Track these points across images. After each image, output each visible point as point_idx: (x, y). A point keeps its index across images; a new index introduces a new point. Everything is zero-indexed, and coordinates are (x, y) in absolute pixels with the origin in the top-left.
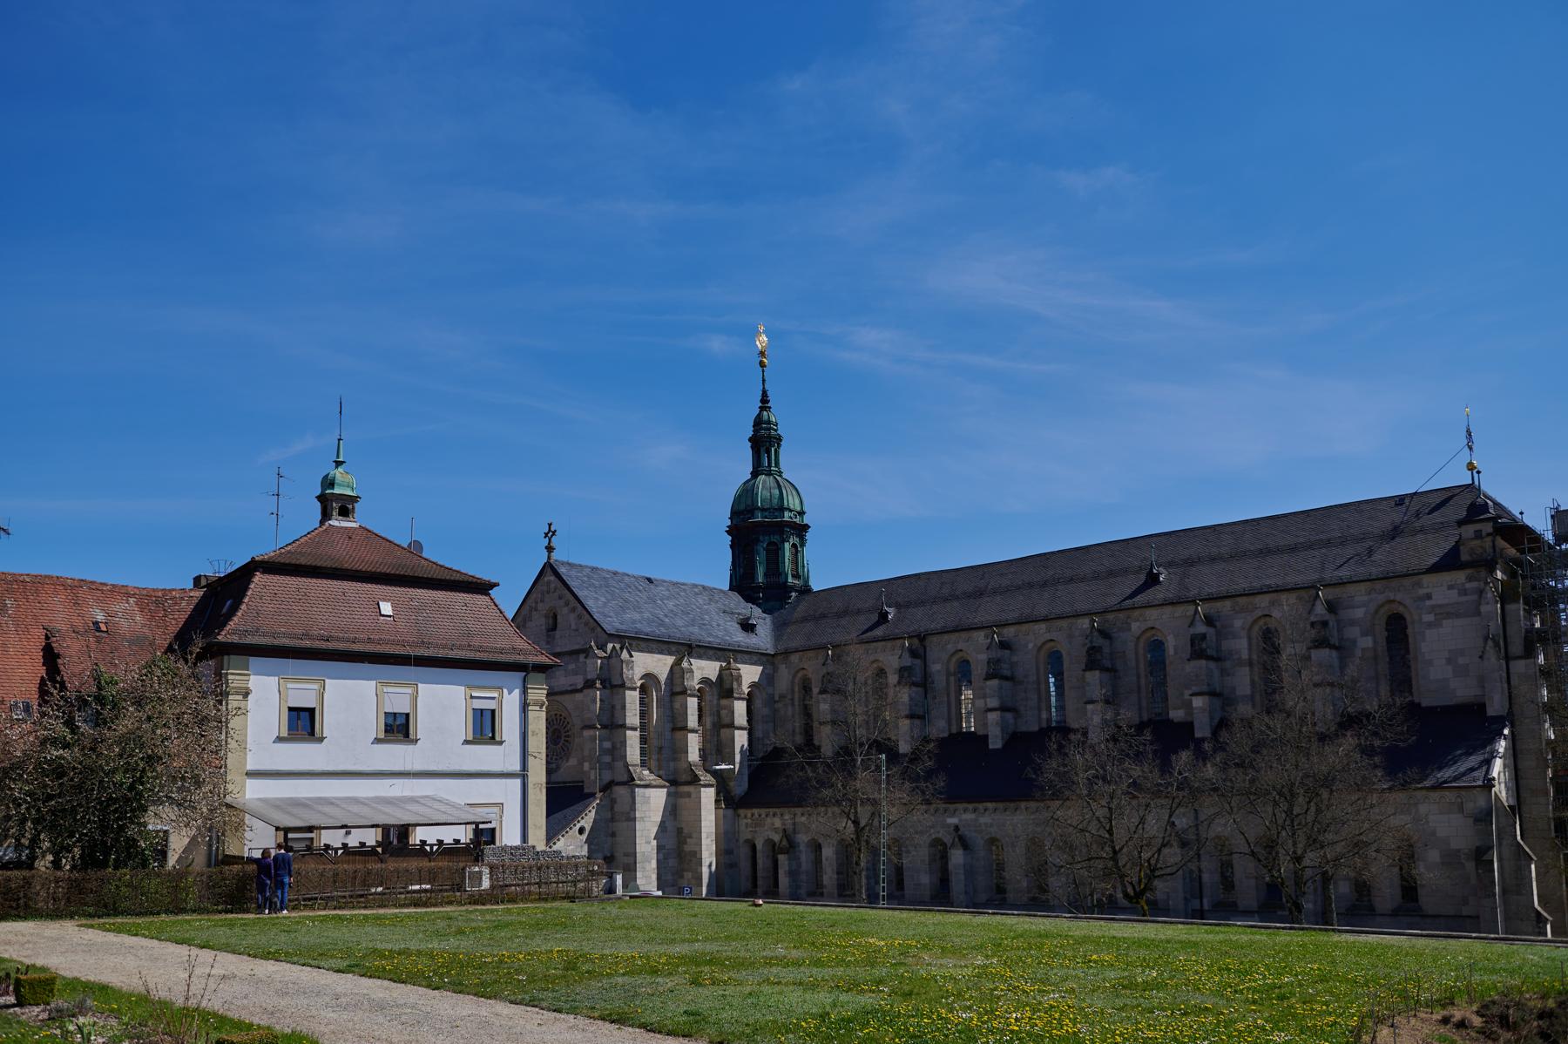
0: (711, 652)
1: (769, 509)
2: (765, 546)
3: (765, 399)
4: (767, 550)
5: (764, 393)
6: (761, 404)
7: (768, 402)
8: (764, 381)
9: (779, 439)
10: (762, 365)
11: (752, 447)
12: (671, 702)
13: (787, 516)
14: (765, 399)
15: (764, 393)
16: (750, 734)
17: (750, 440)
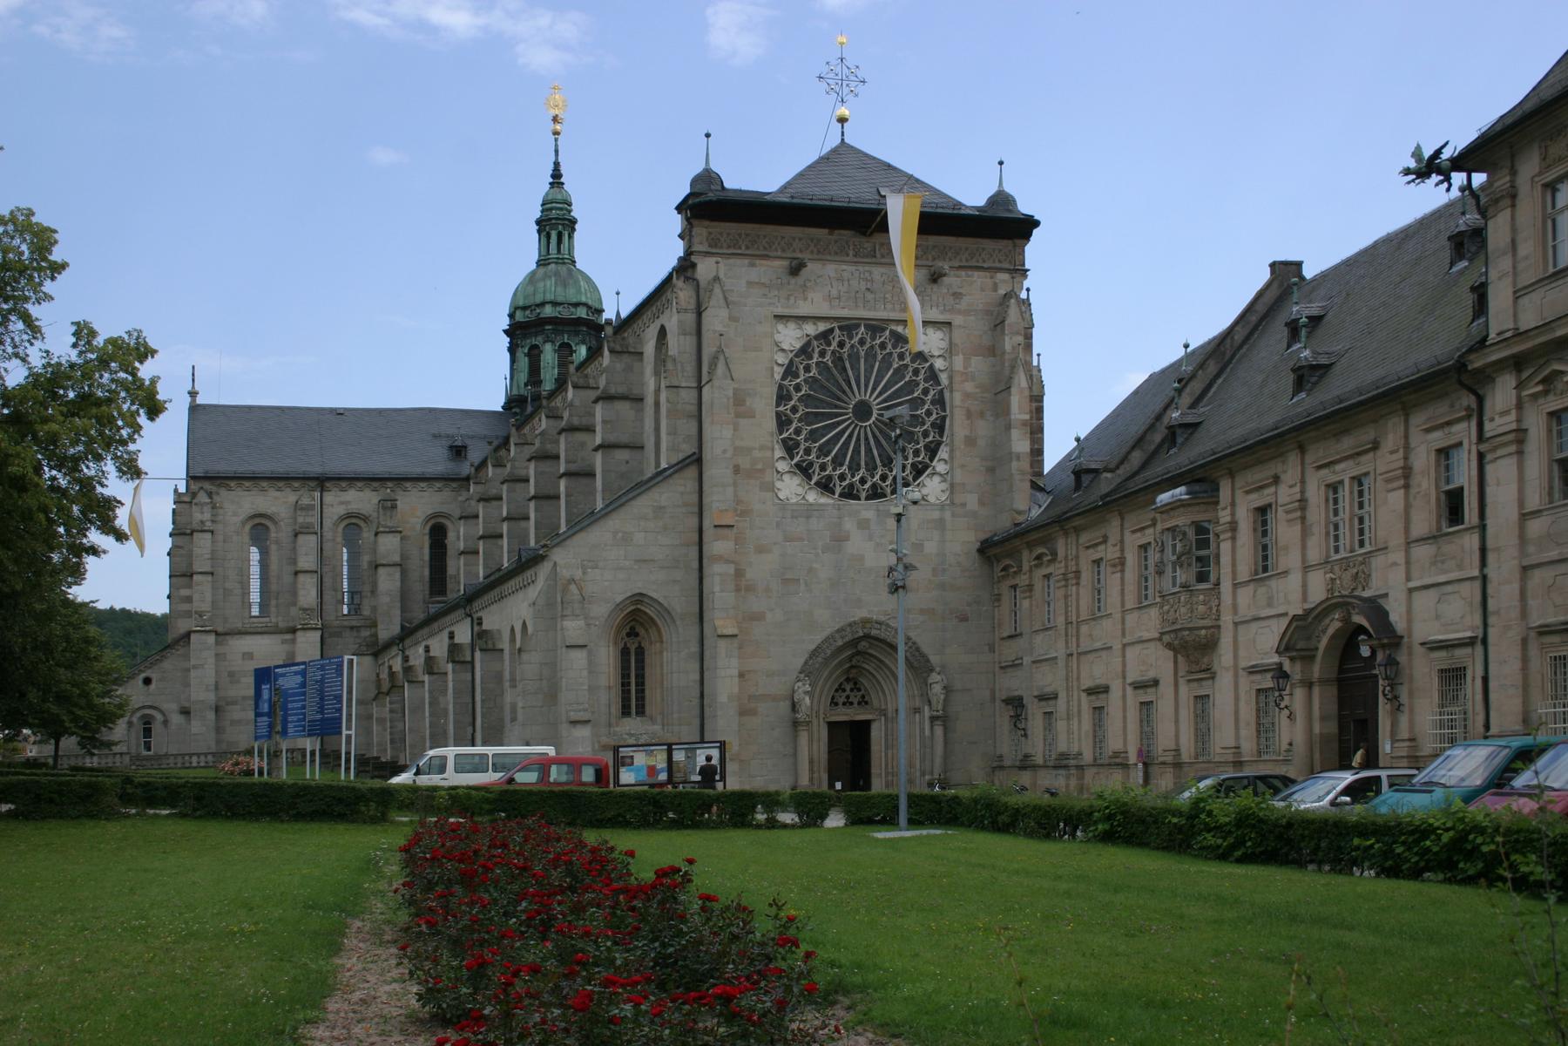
0: (359, 484)
1: (530, 307)
2: (526, 351)
3: (557, 175)
4: (529, 355)
5: (557, 165)
6: (551, 180)
7: (560, 176)
8: (557, 152)
9: (573, 222)
10: (556, 133)
11: (539, 232)
12: (295, 542)
13: (548, 311)
14: (557, 175)
15: (557, 165)
16: (404, 573)
17: (538, 222)
